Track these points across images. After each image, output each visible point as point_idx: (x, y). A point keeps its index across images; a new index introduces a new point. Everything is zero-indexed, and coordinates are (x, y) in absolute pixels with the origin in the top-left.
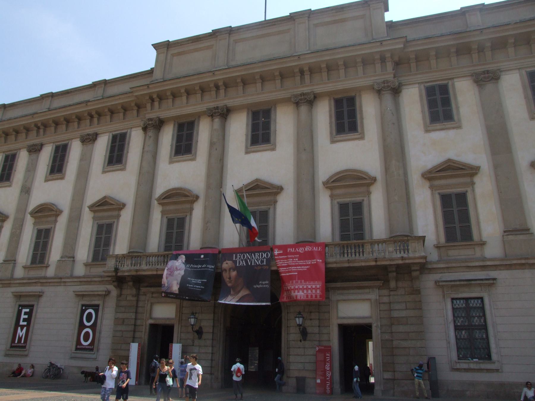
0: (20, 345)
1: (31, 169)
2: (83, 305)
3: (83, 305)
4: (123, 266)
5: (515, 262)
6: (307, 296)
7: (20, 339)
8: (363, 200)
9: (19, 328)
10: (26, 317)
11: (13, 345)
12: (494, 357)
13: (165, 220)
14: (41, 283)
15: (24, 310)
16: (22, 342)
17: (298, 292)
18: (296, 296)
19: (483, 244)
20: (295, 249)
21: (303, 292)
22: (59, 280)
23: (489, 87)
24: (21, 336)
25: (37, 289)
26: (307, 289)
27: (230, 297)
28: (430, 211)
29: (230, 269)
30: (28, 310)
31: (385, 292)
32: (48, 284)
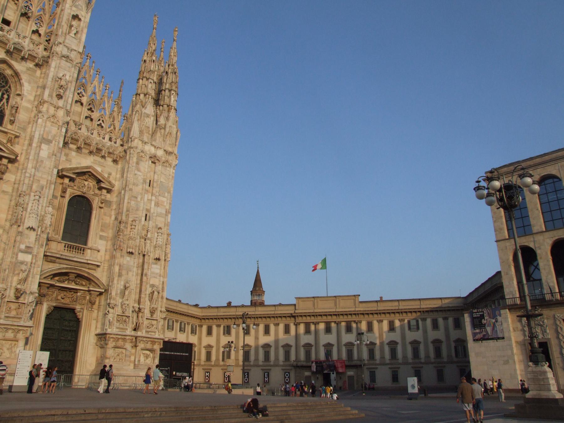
1: (257, 331)
7: (266, 381)
12: (376, 382)
19: (376, 360)
23: (381, 324)
25: (269, 368)
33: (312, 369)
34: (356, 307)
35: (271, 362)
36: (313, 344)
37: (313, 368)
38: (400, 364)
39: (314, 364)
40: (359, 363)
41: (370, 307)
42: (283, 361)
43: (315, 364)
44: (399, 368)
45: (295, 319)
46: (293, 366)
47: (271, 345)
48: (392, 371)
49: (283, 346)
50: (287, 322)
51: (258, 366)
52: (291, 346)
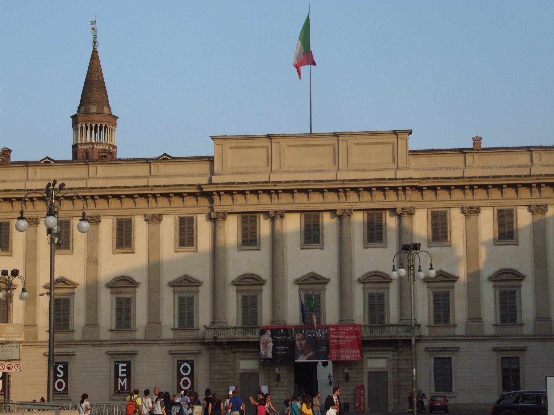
0: (124, 391)
2: (178, 361)
3: (178, 361)
4: (219, 335)
5: (470, 338)
6: (352, 358)
7: (122, 388)
8: (384, 292)
9: (120, 380)
10: (125, 370)
11: (116, 392)
12: (454, 390)
13: (240, 297)
14: (133, 343)
15: (121, 366)
16: (126, 389)
17: (347, 355)
18: (345, 358)
19: (455, 326)
20: (343, 328)
21: (349, 355)
22: (153, 342)
23: (473, 217)
24: (122, 385)
26: (352, 353)
27: (301, 357)
28: (426, 303)
29: (301, 339)
30: (125, 365)
31: (396, 353)
33: (262, 352)
34: (398, 168)
35: (137, 332)
36: (264, 278)
37: (266, 347)
38: (528, 338)
39: (267, 337)
40: (401, 334)
41: (441, 168)
42: (174, 329)
43: (272, 336)
44: (524, 350)
45: (212, 201)
46: (203, 342)
47: (137, 279)
48: (502, 358)
49: (172, 284)
50: (186, 212)
51: (98, 343)
52: (198, 284)
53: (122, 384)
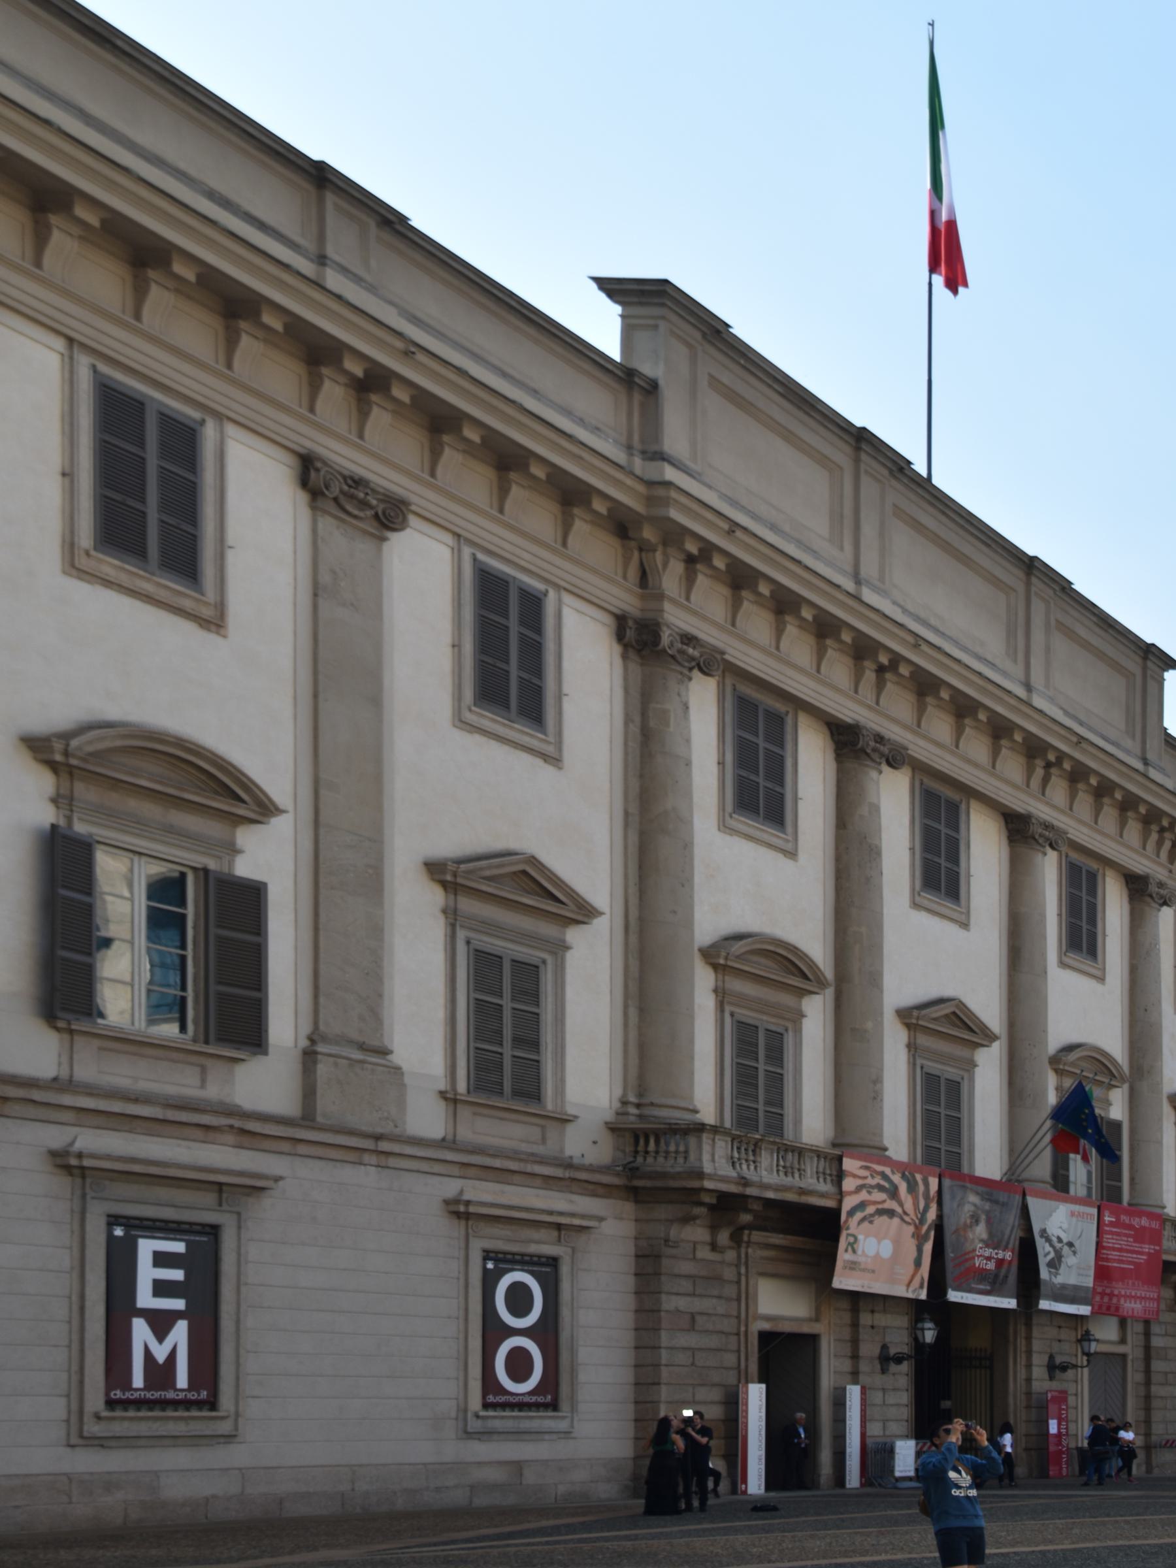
7: (161, 1373)
10: (177, 1275)
11: (118, 1394)
32: (285, 1146)
53: (160, 1353)
